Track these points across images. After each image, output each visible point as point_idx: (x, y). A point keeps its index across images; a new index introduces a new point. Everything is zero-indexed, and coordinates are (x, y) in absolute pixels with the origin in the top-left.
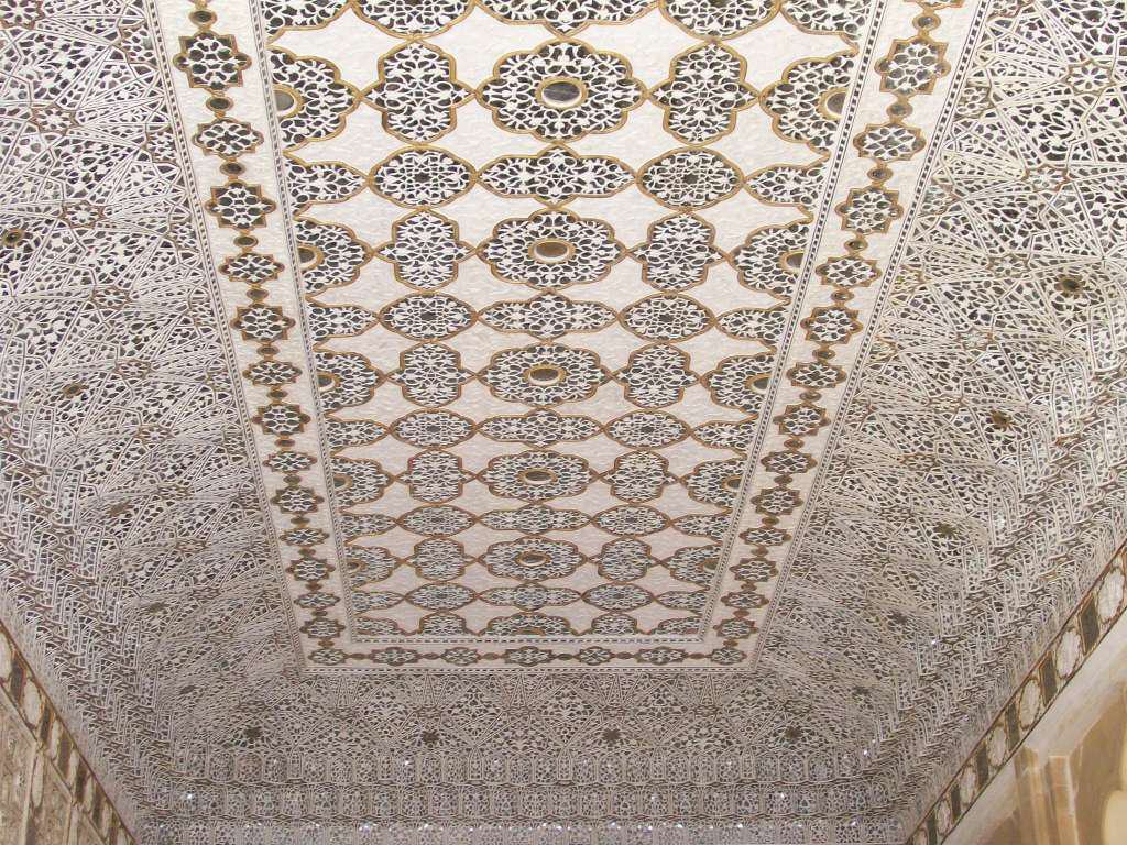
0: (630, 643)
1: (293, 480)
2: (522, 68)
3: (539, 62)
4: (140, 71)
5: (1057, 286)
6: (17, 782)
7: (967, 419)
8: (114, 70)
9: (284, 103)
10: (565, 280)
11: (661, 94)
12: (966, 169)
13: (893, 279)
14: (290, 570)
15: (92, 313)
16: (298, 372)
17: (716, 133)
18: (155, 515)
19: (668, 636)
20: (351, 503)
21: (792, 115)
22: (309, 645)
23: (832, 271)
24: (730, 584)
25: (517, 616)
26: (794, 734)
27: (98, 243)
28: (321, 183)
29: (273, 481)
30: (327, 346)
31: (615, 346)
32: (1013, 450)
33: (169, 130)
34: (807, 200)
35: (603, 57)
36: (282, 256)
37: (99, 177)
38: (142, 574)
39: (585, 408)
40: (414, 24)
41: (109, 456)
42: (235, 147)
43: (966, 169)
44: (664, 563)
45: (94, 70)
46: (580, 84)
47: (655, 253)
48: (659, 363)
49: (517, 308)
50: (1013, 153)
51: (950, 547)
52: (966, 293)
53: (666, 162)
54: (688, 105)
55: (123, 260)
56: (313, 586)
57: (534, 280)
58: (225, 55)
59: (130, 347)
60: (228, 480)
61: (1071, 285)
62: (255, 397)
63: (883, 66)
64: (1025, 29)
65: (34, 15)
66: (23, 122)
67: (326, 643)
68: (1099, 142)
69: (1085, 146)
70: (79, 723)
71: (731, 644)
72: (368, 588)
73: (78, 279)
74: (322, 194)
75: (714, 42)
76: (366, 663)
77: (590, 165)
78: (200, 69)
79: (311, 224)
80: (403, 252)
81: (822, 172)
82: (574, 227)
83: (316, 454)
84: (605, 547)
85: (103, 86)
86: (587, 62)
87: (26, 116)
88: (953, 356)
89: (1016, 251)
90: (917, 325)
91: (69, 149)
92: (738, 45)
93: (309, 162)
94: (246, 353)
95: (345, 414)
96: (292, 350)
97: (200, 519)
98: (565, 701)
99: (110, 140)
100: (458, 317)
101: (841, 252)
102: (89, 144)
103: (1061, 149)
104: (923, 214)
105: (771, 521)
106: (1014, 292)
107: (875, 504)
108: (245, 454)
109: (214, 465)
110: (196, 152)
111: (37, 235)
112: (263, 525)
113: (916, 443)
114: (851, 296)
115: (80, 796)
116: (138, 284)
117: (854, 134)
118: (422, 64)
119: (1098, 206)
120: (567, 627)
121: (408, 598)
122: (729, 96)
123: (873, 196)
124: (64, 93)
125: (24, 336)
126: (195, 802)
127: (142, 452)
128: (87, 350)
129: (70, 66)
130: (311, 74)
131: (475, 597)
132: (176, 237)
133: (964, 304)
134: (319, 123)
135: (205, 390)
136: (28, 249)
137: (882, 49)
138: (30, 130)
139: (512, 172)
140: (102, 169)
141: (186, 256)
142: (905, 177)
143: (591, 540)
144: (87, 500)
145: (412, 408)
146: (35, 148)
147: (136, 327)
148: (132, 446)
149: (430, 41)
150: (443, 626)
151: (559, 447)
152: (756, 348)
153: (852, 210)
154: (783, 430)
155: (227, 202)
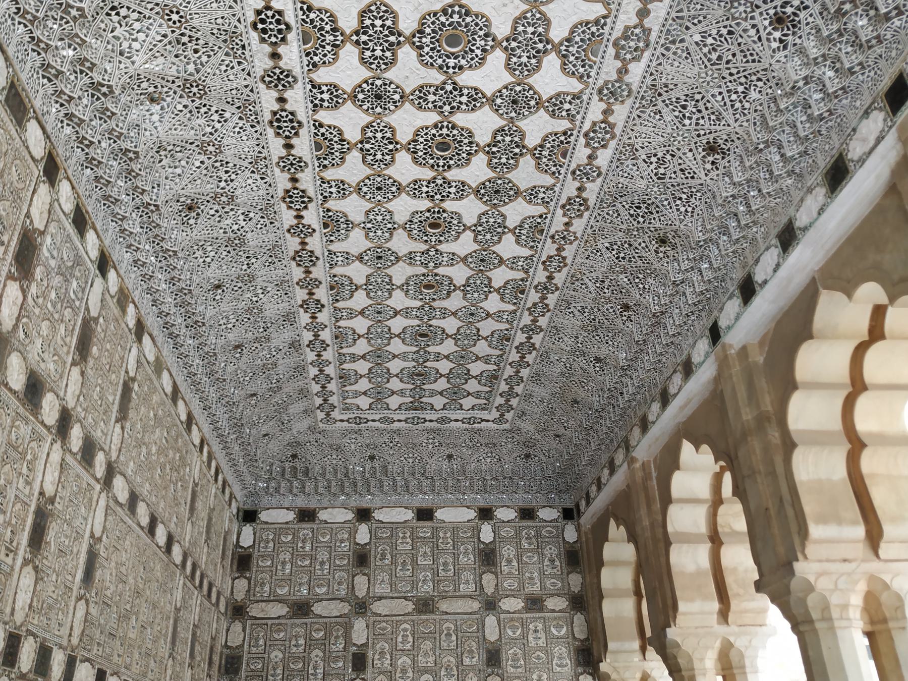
0: (459, 415)
1: (316, 336)
2: (426, 134)
3: (434, 131)
4: (252, 126)
5: (657, 242)
6: (188, 470)
7: (612, 307)
8: (240, 125)
9: (318, 147)
10: (440, 241)
11: (487, 149)
12: (620, 186)
13: (584, 241)
14: (314, 379)
15: (228, 249)
16: (320, 283)
17: (511, 169)
19: (476, 412)
20: (342, 348)
21: (544, 160)
22: (321, 415)
23: (557, 237)
24: (504, 387)
25: (411, 402)
26: (527, 456)
27: (231, 213)
28: (334, 190)
29: (308, 336)
30: (334, 271)
31: (459, 274)
33: (265, 158)
34: (547, 202)
35: (462, 129)
36: (315, 226)
37: (232, 181)
38: (247, 378)
39: (445, 304)
40: (379, 110)
41: (234, 321)
42: (295, 169)
43: (620, 186)
44: (475, 377)
45: (231, 124)
46: (452, 143)
47: (480, 229)
48: (478, 282)
49: (419, 254)
50: (642, 177)
52: (615, 247)
53: (487, 183)
54: (498, 155)
55: (243, 224)
56: (323, 387)
57: (426, 241)
58: (291, 121)
59: (245, 267)
60: (288, 335)
61: (663, 241)
62: (301, 295)
63: (586, 135)
64: (652, 114)
65: (202, 92)
66: (196, 149)
67: (328, 414)
68: (681, 170)
69: (675, 172)
70: (216, 448)
71: (502, 415)
72: (347, 388)
73: (222, 231)
74: (334, 195)
75: (512, 123)
76: (345, 424)
77: (454, 184)
78: (279, 128)
79: (328, 210)
80: (369, 225)
81: (556, 189)
82: (445, 215)
83: (327, 323)
84: (451, 370)
85: (234, 133)
86: (455, 132)
87: (198, 146)
88: (607, 277)
89: (640, 226)
90: (592, 263)
91: (218, 164)
92: (522, 124)
93: (328, 178)
94: (298, 273)
95: (340, 305)
96: (318, 272)
97: (274, 353)
98: (431, 441)
99: (237, 161)
100: (393, 258)
102: (227, 163)
103: (664, 174)
105: (523, 357)
106: (637, 245)
107: (569, 348)
110: (277, 171)
111: (202, 207)
112: (302, 357)
114: (564, 249)
115: (216, 480)
116: (249, 235)
117: (571, 169)
118: (381, 131)
119: (678, 202)
120: (432, 408)
121: (365, 393)
122: (517, 150)
123: (578, 200)
124: (216, 135)
125: (196, 258)
126: (267, 487)
128: (225, 267)
129: (219, 122)
130: (331, 133)
131: (393, 393)
132: (267, 212)
133: (614, 252)
134: (333, 159)
136: (198, 214)
137: (587, 126)
138: (199, 153)
140: (233, 177)
141: (271, 223)
142: (592, 190)
143: (444, 366)
144: (223, 341)
145: (371, 302)
146: (202, 162)
147: (248, 257)
149: (385, 119)
150: (379, 407)
151: (433, 322)
152: (522, 275)
153: (568, 207)
154: (530, 314)
155: (291, 197)
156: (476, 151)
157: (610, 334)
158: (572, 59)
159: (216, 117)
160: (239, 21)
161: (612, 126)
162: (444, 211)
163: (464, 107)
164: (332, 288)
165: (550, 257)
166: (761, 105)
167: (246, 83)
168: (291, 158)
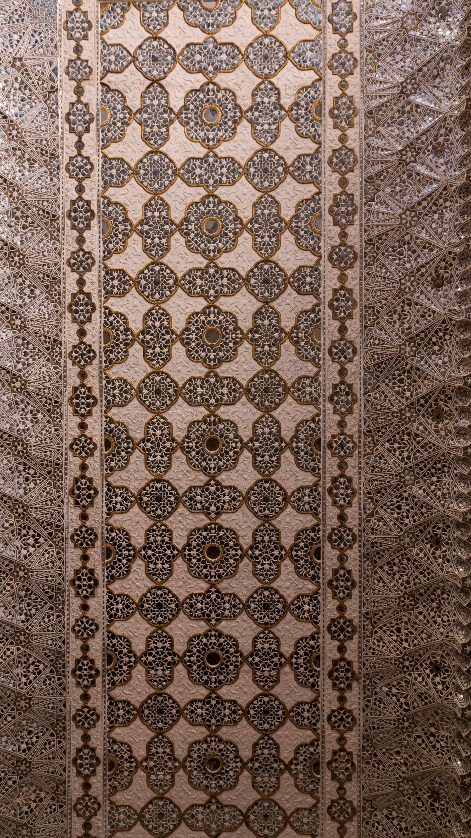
5: (433, 420)
7: (421, 550)
18: (8, 656)
32: (448, 561)
36: (97, 440)
43: (376, 356)
48: (266, 538)
51: (443, 683)
59: (22, 491)
69: (418, 322)
74: (117, 399)
75: (267, 303)
82: (221, 426)
101: (335, 430)
104: (365, 394)
108: (63, 613)
109: (46, 620)
113: (402, 585)
123: (343, 387)
127: (12, 587)
129: (29, 297)
133: (397, 454)
135: (51, 546)
139: (195, 389)
140: (31, 361)
148: (9, 581)
149: (162, 306)
156: (241, 339)
157: (434, 605)
158: (302, 233)
159: (27, 291)
160: (59, 207)
161: (350, 291)
162: (220, 421)
163: (225, 289)
164: (108, 553)
165: (335, 480)
166: (457, 220)
167: (55, 261)
168: (83, 346)
